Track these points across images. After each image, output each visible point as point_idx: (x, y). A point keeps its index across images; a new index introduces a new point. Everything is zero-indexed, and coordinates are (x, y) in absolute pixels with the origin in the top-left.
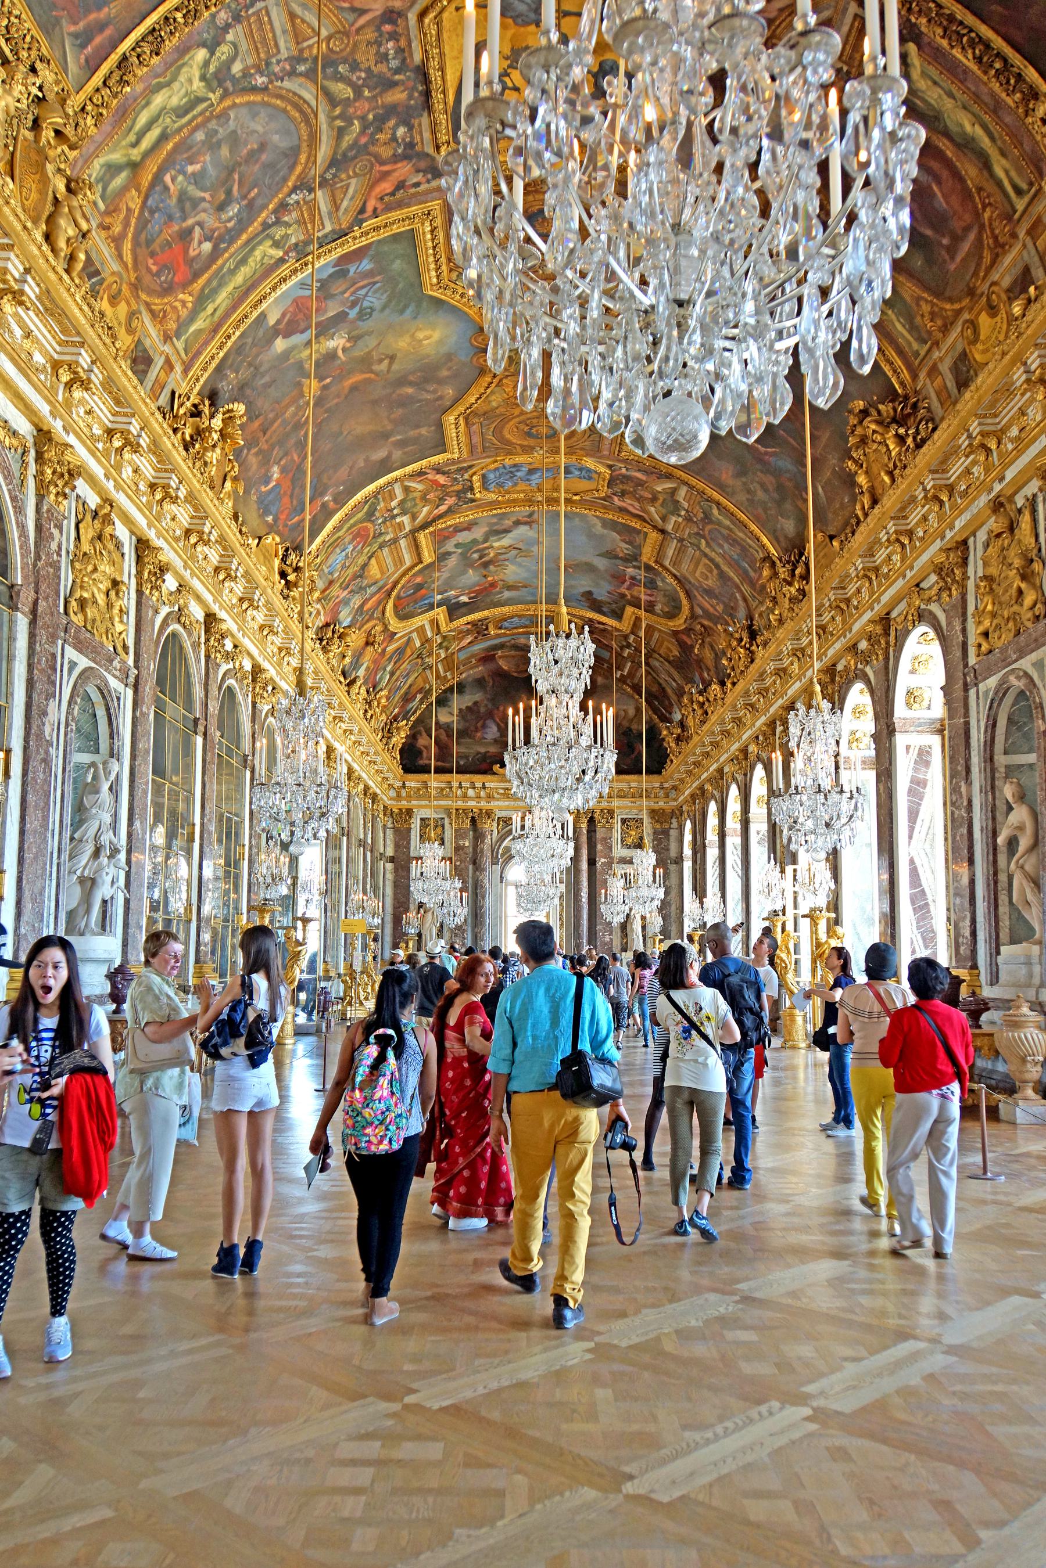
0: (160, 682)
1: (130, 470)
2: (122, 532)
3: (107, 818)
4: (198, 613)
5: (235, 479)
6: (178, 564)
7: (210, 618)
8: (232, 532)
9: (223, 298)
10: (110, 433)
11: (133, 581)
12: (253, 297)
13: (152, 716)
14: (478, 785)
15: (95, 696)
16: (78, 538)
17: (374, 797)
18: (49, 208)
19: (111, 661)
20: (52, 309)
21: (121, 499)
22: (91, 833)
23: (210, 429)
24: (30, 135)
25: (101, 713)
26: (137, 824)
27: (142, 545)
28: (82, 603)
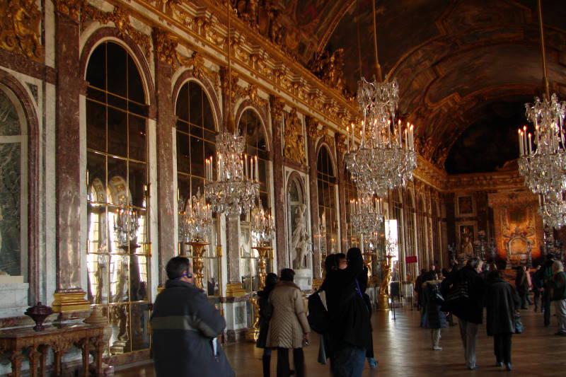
0: (319, 169)
1: (301, 92)
2: (300, 116)
3: (303, 226)
4: (332, 134)
5: (342, 78)
6: (322, 119)
7: (338, 135)
8: (343, 100)
9: (330, 15)
10: (293, 84)
11: (306, 133)
12: (342, 9)
13: (317, 183)
14: (488, 178)
15: (296, 181)
16: (285, 126)
17: (432, 190)
18: (269, 23)
19: (300, 166)
20: (272, 56)
21: (300, 105)
22: (299, 232)
23: (330, 63)
24: (261, 7)
25: (298, 186)
26: (315, 225)
27: (308, 118)
28: (289, 150)
